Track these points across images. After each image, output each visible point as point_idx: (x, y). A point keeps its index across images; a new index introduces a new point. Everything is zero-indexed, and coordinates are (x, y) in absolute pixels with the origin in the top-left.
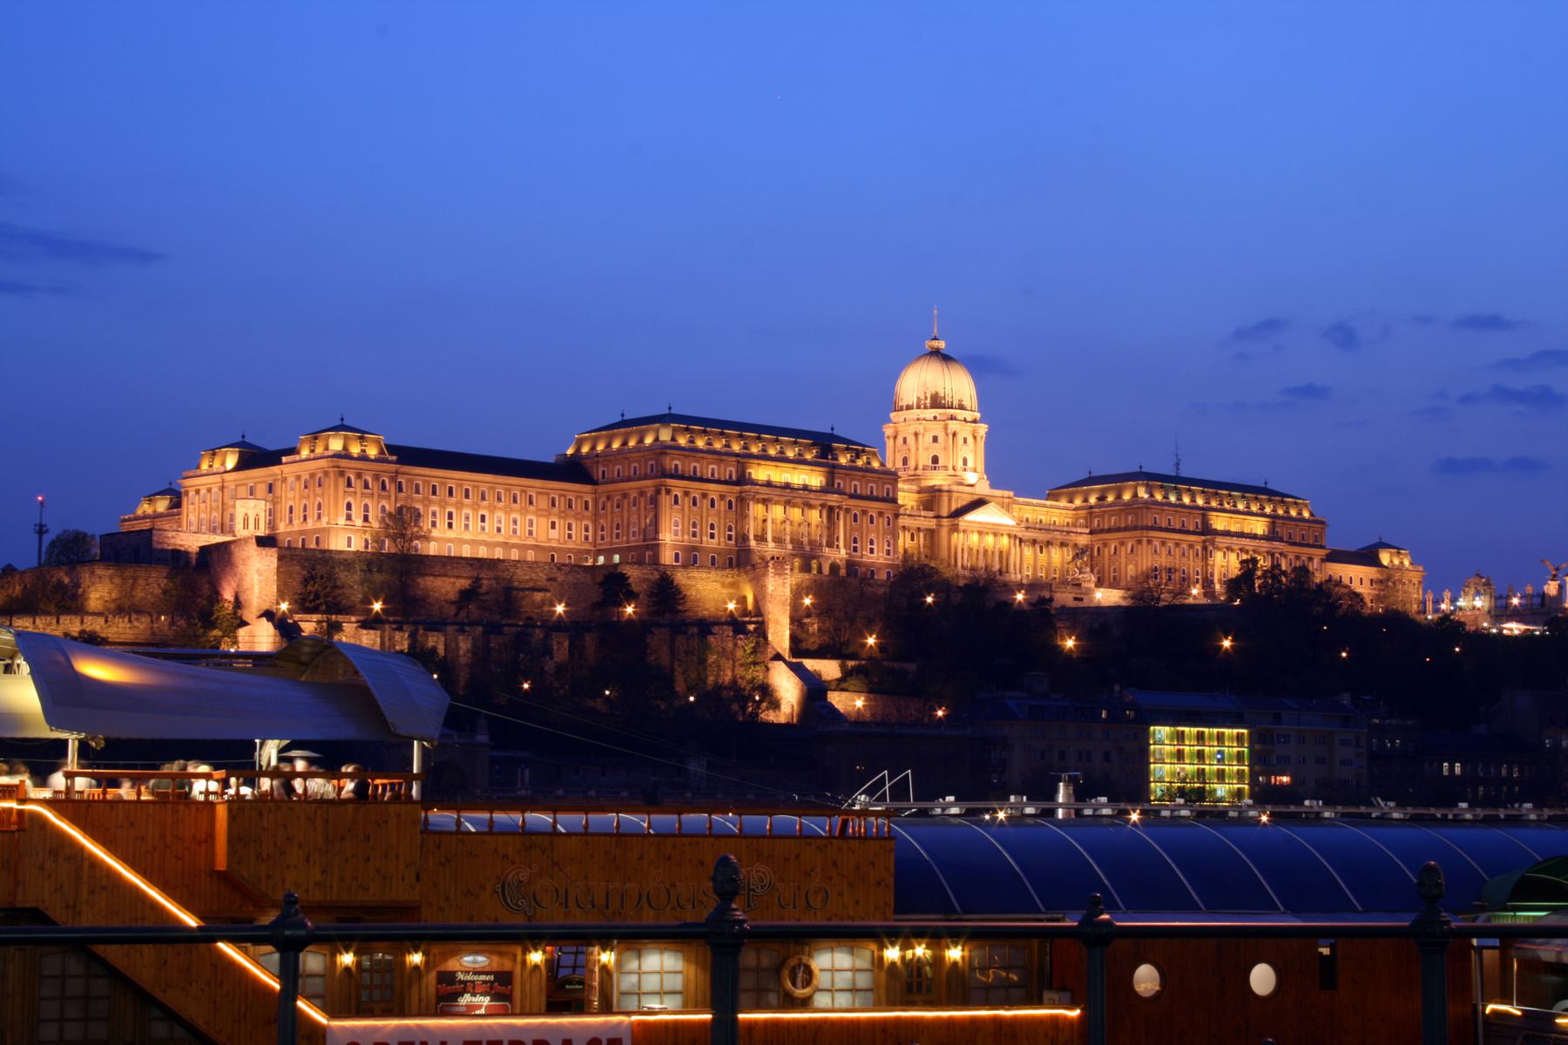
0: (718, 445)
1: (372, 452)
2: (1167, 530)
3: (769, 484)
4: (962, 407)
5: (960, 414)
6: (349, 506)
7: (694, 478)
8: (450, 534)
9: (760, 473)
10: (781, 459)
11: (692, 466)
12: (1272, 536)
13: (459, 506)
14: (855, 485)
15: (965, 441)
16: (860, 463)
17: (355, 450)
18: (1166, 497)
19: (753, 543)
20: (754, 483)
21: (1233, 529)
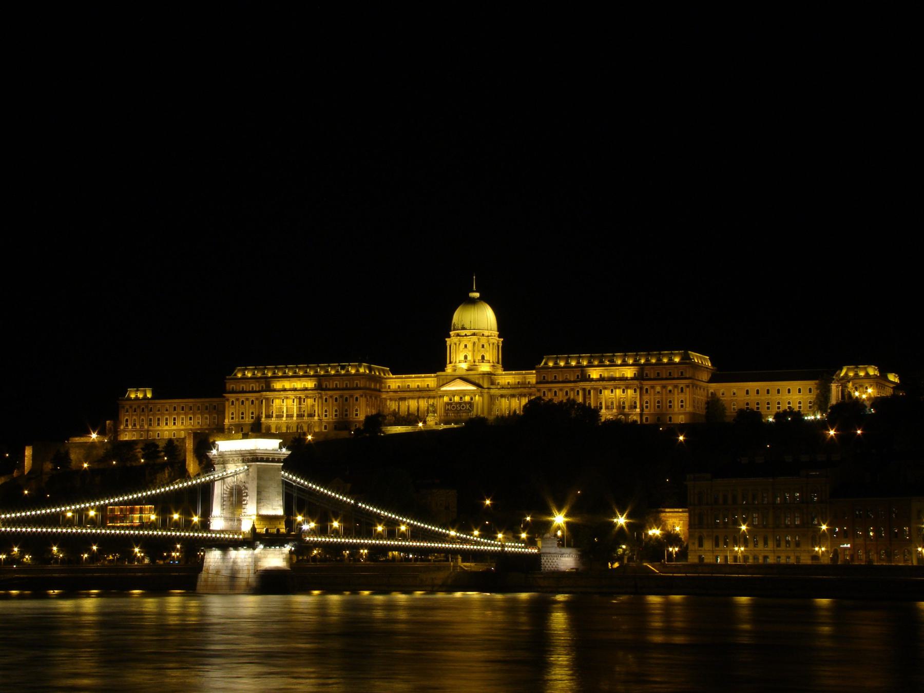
0: (259, 375)
1: (140, 396)
2: (552, 382)
3: (285, 390)
4: (463, 328)
5: (463, 332)
6: (127, 421)
7: (243, 392)
8: (174, 427)
9: (278, 385)
10: (296, 376)
11: (242, 386)
12: (640, 377)
13: (178, 414)
14: (331, 385)
15: (466, 346)
16: (343, 372)
17: (133, 396)
18: (556, 363)
19: (263, 420)
20: (275, 390)
21: (606, 375)
